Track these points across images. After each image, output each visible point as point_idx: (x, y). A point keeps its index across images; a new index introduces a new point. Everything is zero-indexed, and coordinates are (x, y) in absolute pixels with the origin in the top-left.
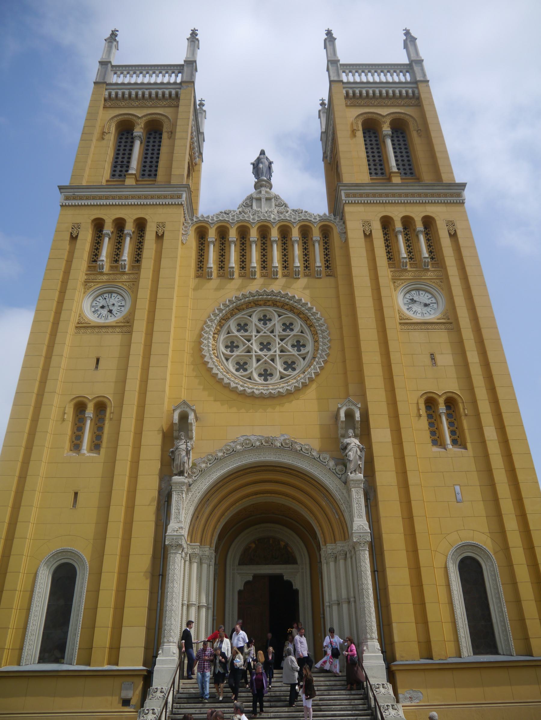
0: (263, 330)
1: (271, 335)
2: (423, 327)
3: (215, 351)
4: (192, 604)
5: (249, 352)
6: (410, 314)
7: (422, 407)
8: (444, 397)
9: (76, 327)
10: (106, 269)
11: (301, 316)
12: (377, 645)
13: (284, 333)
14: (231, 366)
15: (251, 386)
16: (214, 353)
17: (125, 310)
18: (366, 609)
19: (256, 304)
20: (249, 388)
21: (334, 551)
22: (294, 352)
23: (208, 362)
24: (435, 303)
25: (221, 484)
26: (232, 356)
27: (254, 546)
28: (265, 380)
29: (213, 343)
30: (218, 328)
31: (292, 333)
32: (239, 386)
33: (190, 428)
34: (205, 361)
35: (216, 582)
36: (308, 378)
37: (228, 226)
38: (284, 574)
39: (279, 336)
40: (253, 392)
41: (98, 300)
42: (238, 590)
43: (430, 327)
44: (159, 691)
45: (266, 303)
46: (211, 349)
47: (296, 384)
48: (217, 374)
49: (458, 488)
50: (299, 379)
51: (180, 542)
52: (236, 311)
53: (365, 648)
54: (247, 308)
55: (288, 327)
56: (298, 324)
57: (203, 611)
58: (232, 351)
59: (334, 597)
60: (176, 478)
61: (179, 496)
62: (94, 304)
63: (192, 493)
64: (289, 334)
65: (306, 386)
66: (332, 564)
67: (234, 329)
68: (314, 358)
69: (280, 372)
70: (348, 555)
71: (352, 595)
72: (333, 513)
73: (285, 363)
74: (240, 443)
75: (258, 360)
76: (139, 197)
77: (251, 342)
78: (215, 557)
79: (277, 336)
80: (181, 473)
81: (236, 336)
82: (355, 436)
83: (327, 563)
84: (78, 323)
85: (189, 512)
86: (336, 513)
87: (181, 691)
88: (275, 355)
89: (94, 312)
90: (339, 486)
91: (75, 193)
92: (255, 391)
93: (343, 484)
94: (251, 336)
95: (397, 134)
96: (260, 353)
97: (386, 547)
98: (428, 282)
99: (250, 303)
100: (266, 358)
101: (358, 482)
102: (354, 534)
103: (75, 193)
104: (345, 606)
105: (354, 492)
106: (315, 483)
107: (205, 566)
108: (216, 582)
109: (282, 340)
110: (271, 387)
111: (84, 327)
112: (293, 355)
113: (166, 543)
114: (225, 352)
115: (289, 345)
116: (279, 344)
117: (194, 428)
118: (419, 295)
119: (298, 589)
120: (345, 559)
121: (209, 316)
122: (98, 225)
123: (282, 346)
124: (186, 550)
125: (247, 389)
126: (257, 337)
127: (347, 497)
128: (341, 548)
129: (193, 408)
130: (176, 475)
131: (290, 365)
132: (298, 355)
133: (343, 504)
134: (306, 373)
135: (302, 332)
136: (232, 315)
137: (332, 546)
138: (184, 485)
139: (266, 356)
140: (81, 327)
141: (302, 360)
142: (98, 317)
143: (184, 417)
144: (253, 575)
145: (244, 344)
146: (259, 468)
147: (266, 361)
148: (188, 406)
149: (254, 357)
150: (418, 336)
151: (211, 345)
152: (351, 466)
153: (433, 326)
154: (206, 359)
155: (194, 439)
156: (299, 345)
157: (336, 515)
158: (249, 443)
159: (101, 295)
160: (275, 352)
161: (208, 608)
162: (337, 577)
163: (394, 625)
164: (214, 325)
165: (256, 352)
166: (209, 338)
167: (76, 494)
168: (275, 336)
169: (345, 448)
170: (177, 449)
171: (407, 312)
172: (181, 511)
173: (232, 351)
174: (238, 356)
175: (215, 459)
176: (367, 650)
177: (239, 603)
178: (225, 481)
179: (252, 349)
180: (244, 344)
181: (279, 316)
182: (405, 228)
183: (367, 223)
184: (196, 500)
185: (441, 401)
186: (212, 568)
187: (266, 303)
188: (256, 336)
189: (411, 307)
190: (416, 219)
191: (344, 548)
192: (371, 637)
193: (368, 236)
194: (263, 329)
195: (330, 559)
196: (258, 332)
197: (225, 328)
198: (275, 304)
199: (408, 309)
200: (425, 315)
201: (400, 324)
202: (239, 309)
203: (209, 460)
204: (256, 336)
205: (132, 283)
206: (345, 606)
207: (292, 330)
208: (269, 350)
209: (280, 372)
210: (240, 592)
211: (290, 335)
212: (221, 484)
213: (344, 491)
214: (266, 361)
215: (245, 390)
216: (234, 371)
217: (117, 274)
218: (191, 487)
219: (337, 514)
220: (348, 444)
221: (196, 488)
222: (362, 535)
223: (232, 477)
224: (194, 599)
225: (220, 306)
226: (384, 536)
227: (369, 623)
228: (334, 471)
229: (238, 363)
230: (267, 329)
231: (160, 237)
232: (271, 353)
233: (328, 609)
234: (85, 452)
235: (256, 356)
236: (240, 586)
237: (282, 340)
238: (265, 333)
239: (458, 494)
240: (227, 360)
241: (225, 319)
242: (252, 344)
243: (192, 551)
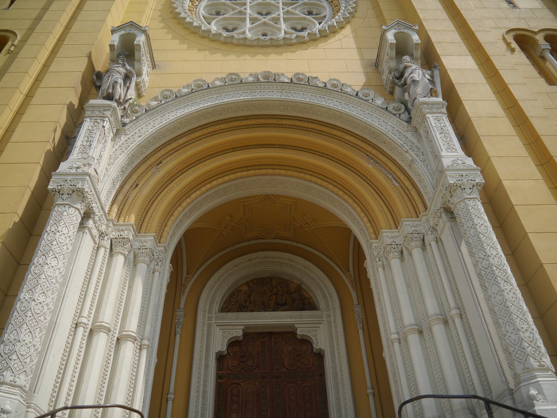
4: (102, 328)
18: (509, 304)
21: (396, 240)
27: (245, 288)
42: (217, 351)
51: (79, 186)
57: (128, 349)
59: (408, 318)
61: (96, 124)
63: (128, 137)
65: (326, 36)
70: (430, 238)
71: (452, 304)
72: (389, 178)
74: (222, 78)
85: (116, 162)
86: (393, 179)
90: (397, 129)
93: (406, 124)
101: (435, 106)
102: (447, 172)
105: (431, 119)
119: (323, 348)
127: (415, 141)
128: (413, 229)
133: (410, 151)
137: (392, 232)
138: (109, 110)
144: (243, 327)
157: (394, 182)
158: (235, 79)
161: (140, 346)
172: (94, 144)
175: (176, 96)
176: (540, 397)
177: (219, 377)
184: (133, 146)
185: (540, 38)
191: (418, 229)
192: (541, 365)
195: (391, 255)
206: (438, 330)
210: (220, 358)
213: (409, 135)
218: (126, 128)
219: (395, 180)
221: (136, 131)
222: (464, 173)
227: (527, 334)
233: (396, 345)
243: (118, 233)
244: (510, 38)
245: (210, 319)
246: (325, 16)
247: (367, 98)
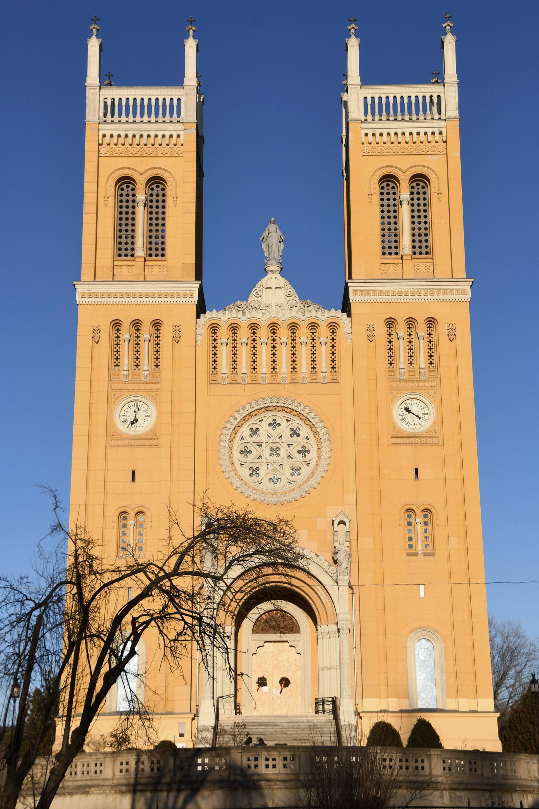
2: (412, 440)
6: (403, 426)
11: (308, 422)
14: (245, 472)
22: (299, 457)
43: (418, 440)
55: (295, 433)
56: (304, 431)
62: (122, 414)
76: (153, 295)
89: (123, 422)
91: (91, 289)
95: (418, 189)
103: (91, 289)
122: (116, 324)
131: (296, 470)
136: (245, 421)
142: (128, 427)
150: (406, 451)
156: (304, 451)
181: (288, 421)
189: (404, 418)
198: (283, 409)
199: (401, 420)
228: (328, 571)
247: (320, 562)
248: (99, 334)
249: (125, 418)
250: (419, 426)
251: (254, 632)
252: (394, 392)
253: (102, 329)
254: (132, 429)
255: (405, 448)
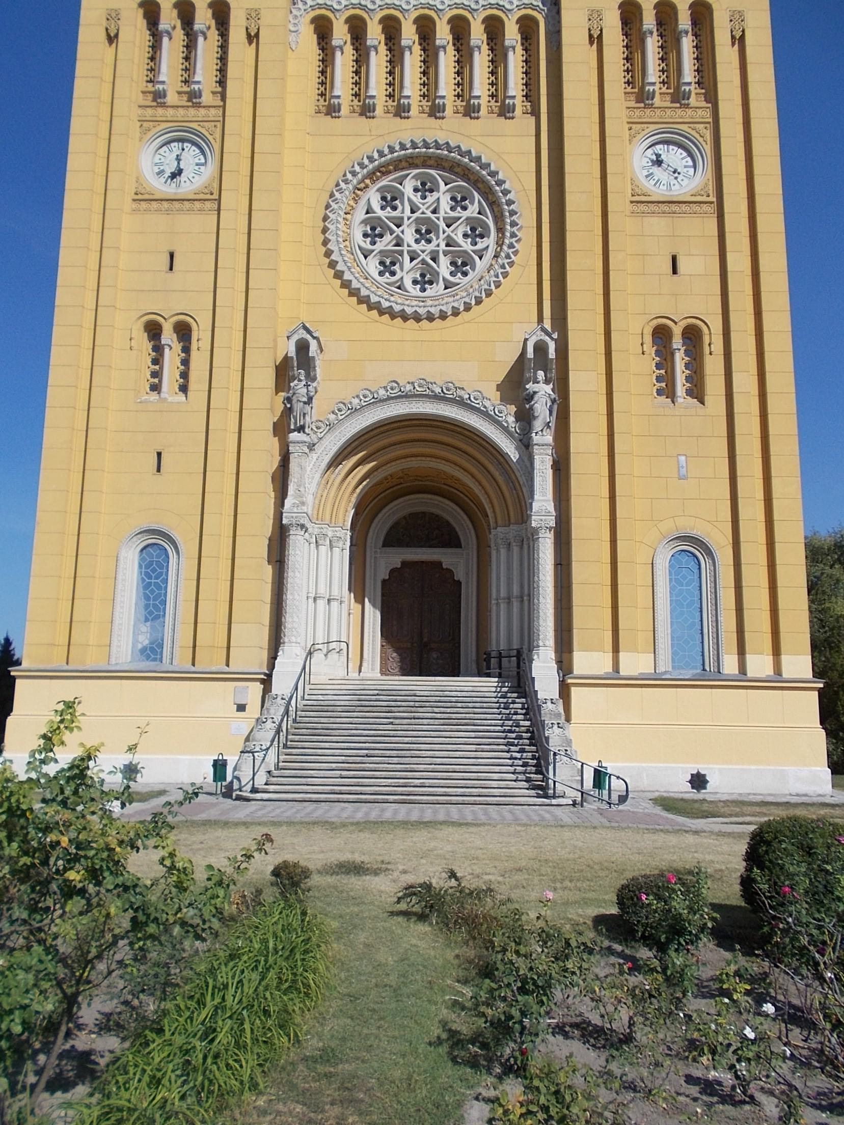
0: (419, 209)
1: (433, 216)
3: (347, 243)
5: (397, 245)
6: (649, 185)
7: (648, 339)
8: (683, 324)
9: (134, 200)
10: (172, 98)
12: (552, 655)
13: (453, 214)
15: (399, 301)
16: (345, 247)
17: (210, 170)
19: (410, 162)
20: (397, 303)
22: (466, 245)
23: (337, 262)
24: (690, 167)
25: (357, 443)
26: (373, 251)
28: (423, 290)
29: (345, 229)
30: (352, 203)
31: (465, 214)
32: (382, 301)
33: (312, 366)
34: (332, 260)
35: (353, 567)
36: (485, 290)
37: (365, 16)
38: (442, 560)
39: (444, 218)
40: (403, 310)
41: (162, 151)
44: (279, 698)
45: (426, 161)
46: (341, 240)
47: (467, 300)
48: (351, 281)
49: (683, 458)
50: (471, 290)
52: (378, 174)
53: (535, 657)
54: (396, 169)
55: (459, 202)
58: (373, 243)
59: (503, 593)
60: (294, 436)
64: (460, 215)
66: (503, 551)
67: (376, 205)
68: (496, 256)
69: (444, 279)
70: (525, 543)
73: (453, 263)
75: (412, 260)
77: (401, 229)
78: (351, 537)
79: (441, 219)
80: (301, 429)
81: (379, 218)
82: (547, 382)
83: (498, 551)
84: (136, 194)
87: (306, 697)
88: (438, 252)
89: (158, 174)
92: (406, 308)
94: (402, 218)
96: (415, 247)
97: (574, 535)
98: (684, 127)
99: (400, 161)
100: (423, 256)
104: (516, 605)
106: (487, 445)
107: (336, 551)
108: (353, 567)
109: (448, 226)
110: (429, 303)
111: (145, 200)
112: (465, 252)
113: (285, 521)
114: (363, 245)
115: (460, 235)
116: (444, 232)
117: (318, 363)
118: (668, 151)
120: (521, 547)
121: (337, 185)
123: (449, 236)
124: (310, 530)
125: (394, 305)
126: (411, 220)
129: (315, 335)
130: (294, 430)
132: (474, 251)
134: (482, 282)
135: (479, 213)
139: (423, 252)
140: (140, 200)
141: (477, 258)
142: (166, 182)
143: (303, 347)
145: (392, 232)
146: (410, 423)
147: (423, 260)
148: (309, 331)
149: (405, 253)
150: (657, 225)
151: (340, 233)
152: (538, 425)
153: (684, 207)
154: (333, 257)
155: (319, 378)
159: (167, 143)
160: (438, 245)
162: (509, 568)
163: (575, 631)
164: (344, 199)
165: (408, 246)
166: (338, 222)
167: (159, 455)
168: (438, 219)
169: (530, 397)
170: (294, 394)
171: (643, 180)
173: (373, 243)
174: (381, 252)
177: (383, 595)
178: (363, 438)
179: (402, 240)
180: (392, 232)
182: (660, 24)
183: (595, 15)
185: (677, 331)
186: (347, 553)
187: (426, 161)
188: (409, 218)
189: (652, 174)
190: (679, 7)
193: (596, 40)
194: (421, 206)
196: (413, 212)
197: (363, 203)
198: (439, 163)
199: (647, 176)
200: (673, 188)
201: (632, 202)
202: (383, 171)
203: (340, 410)
204: (409, 218)
205: (213, 124)
206: (516, 605)
207: (465, 208)
208: (429, 241)
209: (444, 279)
210: (384, 582)
211: (459, 218)
212: (357, 443)
214: (423, 260)
215: (391, 307)
216: (376, 276)
217: (188, 107)
220: (535, 393)
223: (372, 434)
224: (322, 590)
225: (353, 167)
226: (574, 521)
229: (382, 263)
230: (426, 206)
231: (253, 38)
232: (431, 247)
234: (167, 396)
235: (408, 252)
236: (384, 574)
237: (448, 226)
238: (423, 213)
239: (682, 467)
240: (366, 257)
241: (361, 188)
242: (402, 232)
244: (648, 331)
245: (376, 552)
246: (488, 247)
248: (119, 22)
249: (162, 168)
250: (677, 187)
251: (386, 544)
252: (634, 126)
253: (124, 15)
254: (173, 185)
255: (654, 220)
